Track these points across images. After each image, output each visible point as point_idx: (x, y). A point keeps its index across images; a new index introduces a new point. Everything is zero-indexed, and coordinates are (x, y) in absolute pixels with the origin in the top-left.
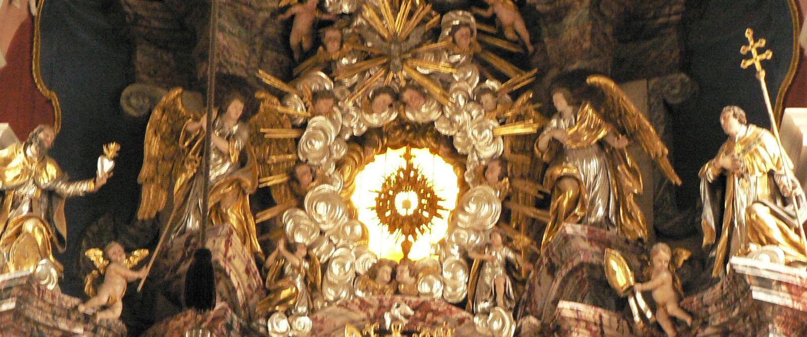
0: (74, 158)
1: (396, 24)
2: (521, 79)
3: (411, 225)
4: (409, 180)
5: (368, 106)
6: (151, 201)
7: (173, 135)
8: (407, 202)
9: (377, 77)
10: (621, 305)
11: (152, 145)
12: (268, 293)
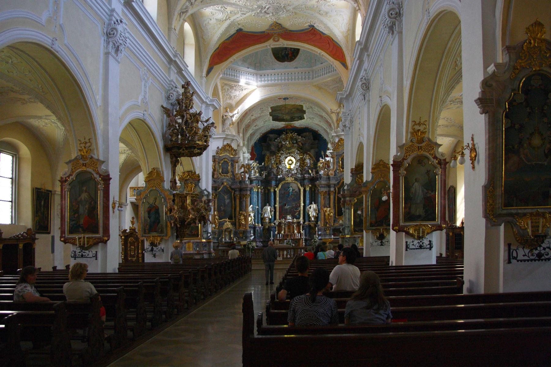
0: (260, 164)
1: (289, 146)
2: (301, 151)
3: (291, 164)
4: (291, 160)
5: (287, 154)
6: (266, 165)
7: (268, 158)
8: (290, 162)
9: (288, 151)
10: (310, 174)
11: (266, 159)
12: (278, 174)
